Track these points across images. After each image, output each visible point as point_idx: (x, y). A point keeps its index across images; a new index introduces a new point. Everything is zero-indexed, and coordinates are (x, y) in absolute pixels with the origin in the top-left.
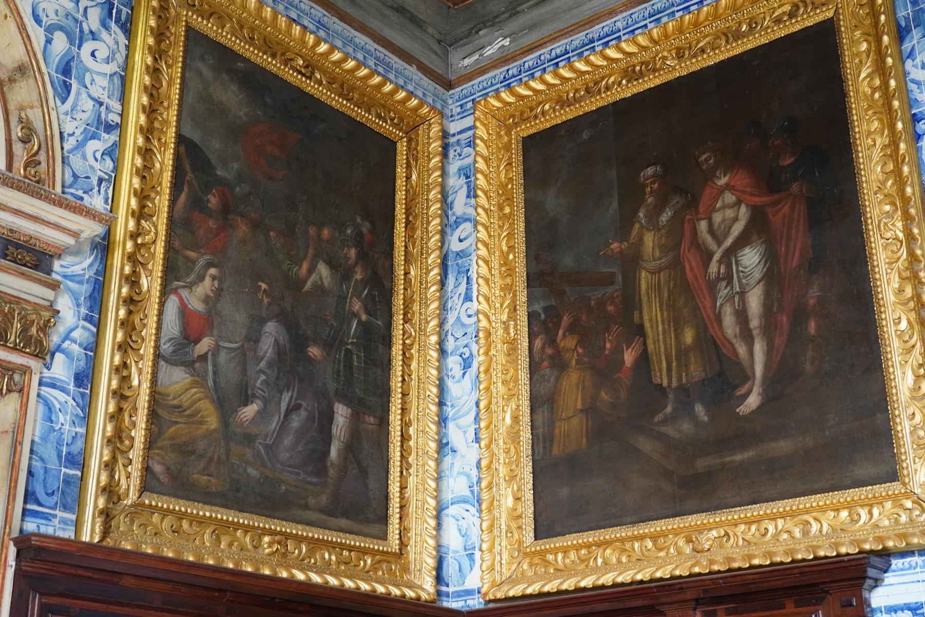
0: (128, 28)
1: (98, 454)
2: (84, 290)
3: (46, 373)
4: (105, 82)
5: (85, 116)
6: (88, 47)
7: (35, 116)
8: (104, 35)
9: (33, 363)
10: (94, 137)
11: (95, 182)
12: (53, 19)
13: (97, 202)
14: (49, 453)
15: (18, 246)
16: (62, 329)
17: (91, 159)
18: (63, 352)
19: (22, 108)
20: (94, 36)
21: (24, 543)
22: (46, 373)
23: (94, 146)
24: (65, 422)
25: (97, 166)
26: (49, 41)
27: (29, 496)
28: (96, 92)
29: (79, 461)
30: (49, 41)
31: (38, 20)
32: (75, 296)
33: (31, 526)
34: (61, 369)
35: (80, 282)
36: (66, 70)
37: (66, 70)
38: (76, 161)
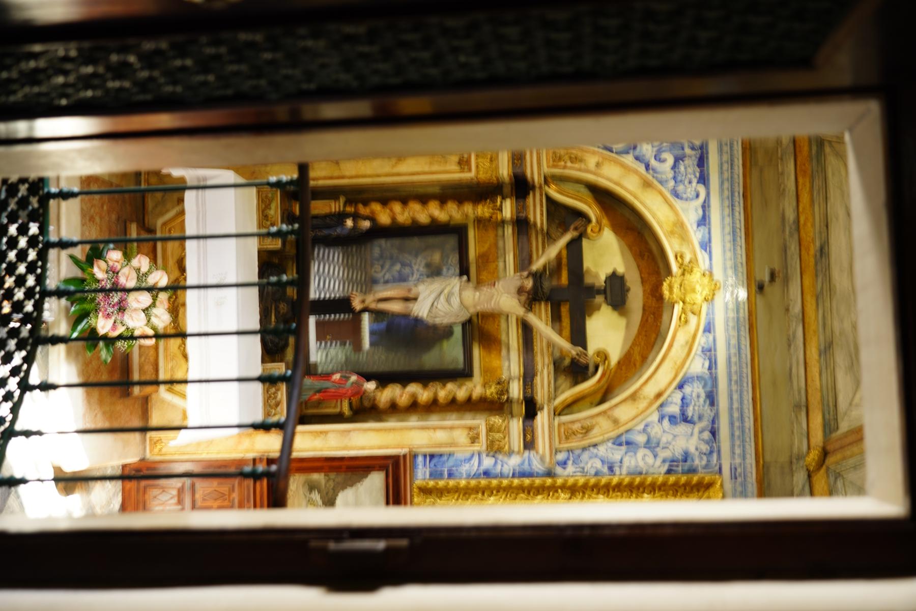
0: (669, 472)
1: (452, 483)
2: (526, 467)
3: (484, 455)
4: (633, 463)
5: (610, 455)
6: (647, 452)
7: (595, 431)
8: (658, 462)
9: (484, 447)
10: (603, 462)
11: (582, 465)
12: (653, 434)
13: (570, 469)
14: (451, 462)
15: (533, 431)
16: (506, 459)
17: (592, 464)
18: (496, 463)
19: (597, 423)
20: (655, 456)
21: (415, 456)
22: (484, 455)
23: (598, 465)
24: (465, 469)
25: (589, 465)
26: (640, 432)
27: (432, 456)
28: (626, 460)
29: (450, 475)
30: (640, 432)
31: (646, 426)
32: (523, 463)
33: (420, 459)
34: (488, 462)
35: (529, 465)
36: (628, 443)
37: (628, 443)
38: (585, 456)
